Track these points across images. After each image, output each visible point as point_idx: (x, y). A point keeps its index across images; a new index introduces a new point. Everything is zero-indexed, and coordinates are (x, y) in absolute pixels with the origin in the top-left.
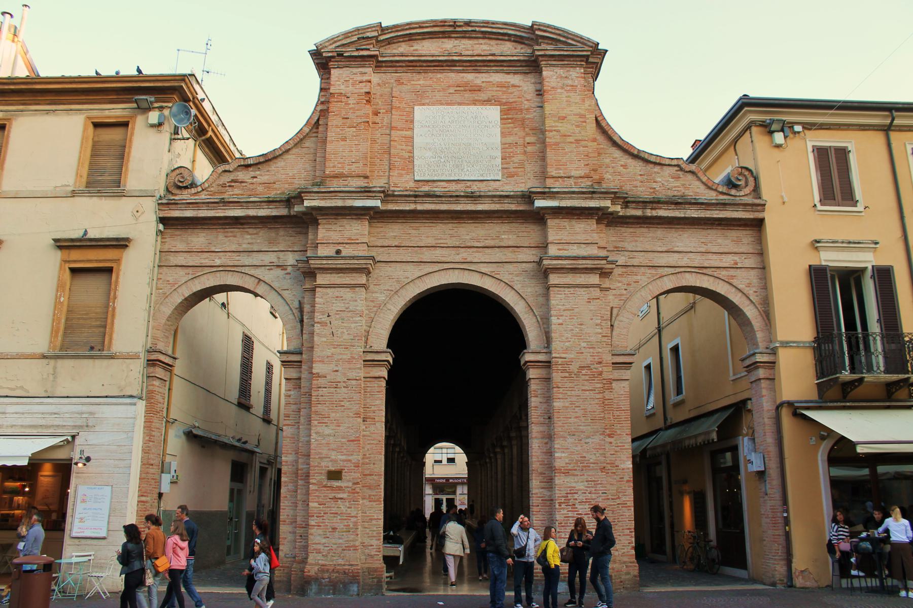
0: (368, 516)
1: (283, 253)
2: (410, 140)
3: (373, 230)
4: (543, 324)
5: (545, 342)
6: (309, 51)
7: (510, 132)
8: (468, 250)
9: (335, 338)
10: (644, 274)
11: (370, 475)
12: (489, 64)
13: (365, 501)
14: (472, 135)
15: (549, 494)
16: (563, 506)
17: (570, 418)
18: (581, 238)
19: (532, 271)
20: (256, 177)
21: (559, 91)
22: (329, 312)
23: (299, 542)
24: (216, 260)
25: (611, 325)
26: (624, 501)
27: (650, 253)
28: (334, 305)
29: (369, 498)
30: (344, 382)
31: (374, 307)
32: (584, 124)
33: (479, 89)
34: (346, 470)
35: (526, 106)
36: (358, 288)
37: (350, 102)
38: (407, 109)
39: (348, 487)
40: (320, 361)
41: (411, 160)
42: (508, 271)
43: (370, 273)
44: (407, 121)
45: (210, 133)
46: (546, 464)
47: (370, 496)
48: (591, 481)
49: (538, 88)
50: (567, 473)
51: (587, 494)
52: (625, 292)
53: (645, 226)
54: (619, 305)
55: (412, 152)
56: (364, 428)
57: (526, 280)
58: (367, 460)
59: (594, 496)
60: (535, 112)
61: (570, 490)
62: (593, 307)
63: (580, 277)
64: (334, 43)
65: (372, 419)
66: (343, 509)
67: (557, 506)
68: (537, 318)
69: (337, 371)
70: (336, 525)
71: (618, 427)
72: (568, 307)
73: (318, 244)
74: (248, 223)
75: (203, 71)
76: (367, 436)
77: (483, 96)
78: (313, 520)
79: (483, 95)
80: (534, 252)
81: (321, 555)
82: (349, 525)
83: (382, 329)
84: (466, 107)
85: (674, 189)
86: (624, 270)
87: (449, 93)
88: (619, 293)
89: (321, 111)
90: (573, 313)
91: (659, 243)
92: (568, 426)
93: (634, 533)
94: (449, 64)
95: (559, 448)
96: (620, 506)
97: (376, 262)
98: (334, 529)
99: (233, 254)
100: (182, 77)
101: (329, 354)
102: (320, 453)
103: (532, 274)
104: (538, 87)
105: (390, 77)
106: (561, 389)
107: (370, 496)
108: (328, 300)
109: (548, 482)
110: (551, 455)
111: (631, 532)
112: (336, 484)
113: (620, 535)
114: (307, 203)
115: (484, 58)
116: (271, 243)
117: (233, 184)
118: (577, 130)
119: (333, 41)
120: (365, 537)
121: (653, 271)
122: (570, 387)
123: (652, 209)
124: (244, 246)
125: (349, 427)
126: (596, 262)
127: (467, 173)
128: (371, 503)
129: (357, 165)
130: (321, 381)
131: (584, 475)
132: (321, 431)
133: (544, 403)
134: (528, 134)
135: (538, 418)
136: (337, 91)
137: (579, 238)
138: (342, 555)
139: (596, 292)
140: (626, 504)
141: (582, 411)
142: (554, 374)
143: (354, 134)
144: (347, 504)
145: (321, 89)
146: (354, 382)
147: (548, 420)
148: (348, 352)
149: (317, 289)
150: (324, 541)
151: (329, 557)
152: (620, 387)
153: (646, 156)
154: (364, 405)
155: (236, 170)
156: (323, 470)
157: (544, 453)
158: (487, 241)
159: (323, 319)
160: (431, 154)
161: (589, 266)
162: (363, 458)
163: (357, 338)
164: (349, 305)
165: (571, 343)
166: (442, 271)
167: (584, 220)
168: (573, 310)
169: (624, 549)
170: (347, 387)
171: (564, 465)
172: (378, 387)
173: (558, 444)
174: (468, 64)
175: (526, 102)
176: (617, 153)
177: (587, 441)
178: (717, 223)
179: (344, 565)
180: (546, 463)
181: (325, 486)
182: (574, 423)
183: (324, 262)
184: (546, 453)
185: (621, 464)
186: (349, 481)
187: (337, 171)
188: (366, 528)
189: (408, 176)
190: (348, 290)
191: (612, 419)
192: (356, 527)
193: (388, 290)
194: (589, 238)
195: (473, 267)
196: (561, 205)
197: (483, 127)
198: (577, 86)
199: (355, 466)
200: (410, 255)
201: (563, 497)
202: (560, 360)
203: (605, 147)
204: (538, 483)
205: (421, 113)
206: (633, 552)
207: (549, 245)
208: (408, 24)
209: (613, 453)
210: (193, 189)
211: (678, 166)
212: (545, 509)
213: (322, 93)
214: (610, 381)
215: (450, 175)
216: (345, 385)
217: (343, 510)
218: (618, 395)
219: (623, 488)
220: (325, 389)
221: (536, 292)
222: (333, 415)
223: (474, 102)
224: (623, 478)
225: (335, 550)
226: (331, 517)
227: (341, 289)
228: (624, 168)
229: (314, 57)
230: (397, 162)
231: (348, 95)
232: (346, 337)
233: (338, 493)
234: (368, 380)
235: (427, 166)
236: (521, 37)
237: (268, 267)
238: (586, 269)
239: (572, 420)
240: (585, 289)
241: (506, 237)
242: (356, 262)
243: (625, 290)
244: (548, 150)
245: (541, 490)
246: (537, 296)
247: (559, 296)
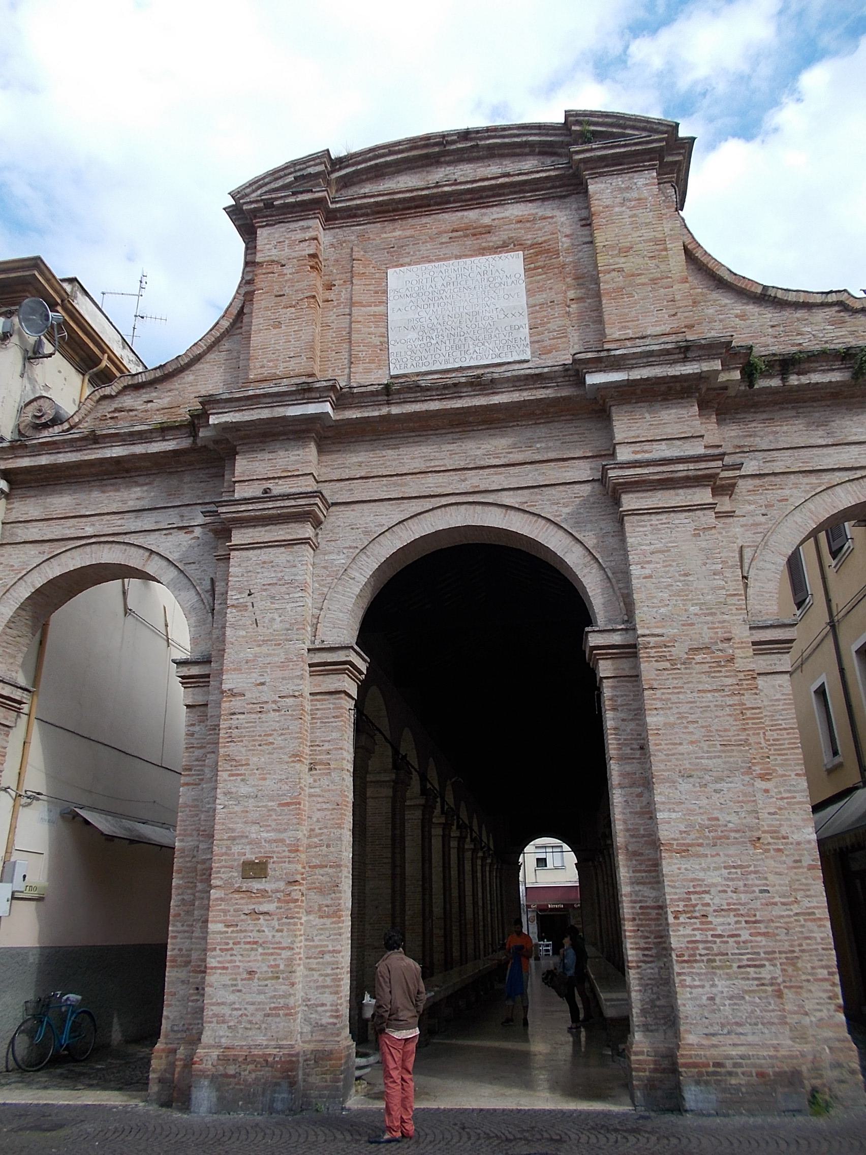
0: (317, 947)
1: (189, 508)
3: (324, 458)
4: (618, 581)
5: (624, 612)
6: (224, 209)
7: (541, 287)
8: (481, 472)
9: (260, 629)
10: (796, 486)
11: (322, 867)
12: (500, 192)
13: (311, 917)
14: (480, 300)
15: (654, 894)
16: (682, 919)
17: (681, 744)
18: (673, 430)
19: (592, 496)
20: (151, 401)
21: (617, 209)
22: (251, 587)
23: (193, 1001)
24: (87, 529)
25: (745, 577)
26: (809, 908)
27: (806, 450)
28: (259, 576)
29: (319, 910)
30: (275, 702)
31: (328, 576)
32: (665, 253)
33: (488, 230)
34: (275, 859)
35: (565, 245)
36: (298, 546)
37: (285, 271)
38: (377, 276)
39: (278, 891)
40: (235, 670)
41: (384, 346)
42: (549, 500)
43: (321, 523)
44: (376, 292)
45: (105, 363)
46: (643, 836)
47: (320, 906)
48: (734, 867)
49: (583, 216)
50: (684, 851)
51: (730, 894)
52: (763, 519)
53: (790, 406)
54: (754, 542)
56: (311, 780)
57: (582, 511)
58: (316, 840)
59: (744, 897)
60: (580, 251)
61: (694, 886)
62: (705, 543)
63: (677, 495)
64: (258, 189)
65: (325, 764)
66: (268, 933)
67: (671, 919)
68: (605, 572)
69: (263, 684)
70: (254, 966)
71: (779, 762)
72: (659, 546)
73: (235, 482)
74: (137, 469)
75: (136, 316)
76: (313, 796)
77: (495, 239)
78: (214, 957)
79: (494, 239)
80: (593, 466)
81: (225, 1026)
82: (278, 966)
83: (341, 612)
84: (468, 260)
86: (757, 482)
87: (442, 243)
88: (751, 522)
89: (246, 294)
90: (669, 556)
91: (820, 433)
92: (677, 759)
93: (837, 977)
94: (439, 200)
95: (663, 803)
96: (801, 918)
97: (329, 506)
98: (251, 973)
99: (114, 517)
100: (33, 262)
101: (251, 657)
102: (233, 830)
103: (591, 499)
104: (584, 214)
105: (350, 234)
106: (659, 692)
107: (320, 906)
108: (250, 568)
109: (650, 871)
110: (651, 818)
111: (830, 974)
112: (256, 885)
113: (808, 981)
114: (213, 420)
115: (493, 182)
116: (170, 495)
117: (116, 415)
118: (652, 264)
119: (257, 185)
120: (310, 988)
121: (813, 479)
122: (675, 688)
123: (798, 374)
124: (131, 503)
125: (281, 780)
126: (703, 465)
127: (474, 356)
128: (322, 920)
129: (297, 360)
130: (237, 704)
131: (718, 854)
132: (234, 790)
133: (632, 720)
135: (620, 749)
136: (267, 259)
137: (669, 430)
138: (263, 1026)
139: (709, 518)
140: (813, 913)
141: (703, 730)
142: (644, 666)
143: (293, 316)
144: (275, 923)
145: (247, 264)
146: (290, 701)
147: (639, 752)
148: (281, 651)
149: (233, 553)
150: (232, 998)
151: (240, 1031)
152: (774, 686)
153: (780, 294)
154: (311, 742)
155: (119, 393)
156: (235, 860)
157: (636, 813)
158: (511, 456)
159: (241, 600)
160: (416, 336)
161: (690, 473)
162: (310, 837)
163: (296, 627)
164: (282, 574)
165: (670, 608)
166: (439, 510)
168: (669, 551)
169: (820, 1010)
170: (278, 711)
171: (678, 836)
172: (334, 708)
173: (661, 794)
174: (469, 196)
175: (564, 239)
176: (725, 300)
177: (718, 786)
179: (267, 1047)
180: (642, 832)
181: (238, 891)
182: (688, 754)
183: (243, 508)
184: (641, 814)
185: (793, 832)
186: (278, 880)
187: (266, 372)
188: (312, 969)
189: (380, 372)
190: (282, 549)
191: (763, 745)
192: (290, 969)
193: (350, 547)
194: (686, 429)
195: (490, 498)
196: (631, 378)
197: (497, 285)
198: (646, 199)
199: (290, 851)
200: (385, 488)
201: (680, 900)
203: (705, 291)
204: (632, 875)
205: (396, 278)
206: (841, 1017)
207: (617, 447)
208: (371, 150)
209: (772, 811)
210: (56, 427)
211: (839, 303)
212: (648, 925)
213: (248, 269)
214: (755, 675)
215: (447, 362)
216: (274, 707)
217: (267, 937)
218: (771, 700)
219: (804, 881)
221: (601, 529)
222: (255, 759)
223: (483, 251)
224: (800, 861)
225: (252, 1015)
226: (247, 950)
227: (270, 549)
228: (744, 320)
229: (234, 217)
230: (362, 352)
231: (283, 262)
232: (277, 626)
233: (260, 903)
234: (318, 697)
235: (409, 353)
237: (165, 532)
238: (687, 478)
240: (687, 514)
241: (543, 445)
242: (293, 503)
243: (763, 515)
244: (604, 302)
245: (637, 888)
246: (603, 537)
247: (641, 529)
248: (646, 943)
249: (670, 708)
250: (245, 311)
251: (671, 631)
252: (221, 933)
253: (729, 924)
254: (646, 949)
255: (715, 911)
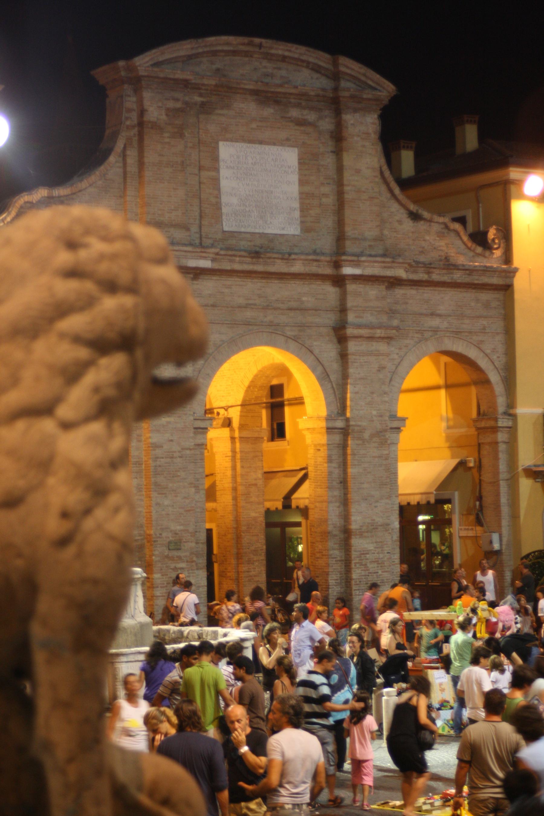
2: (216, 182)
16: (358, 565)
21: (355, 138)
50: (361, 535)
51: (376, 554)
55: (218, 196)
59: (381, 556)
69: (172, 441)
85: (439, 248)
87: (252, 129)
112: (176, 553)
125: (185, 498)
134: (322, 184)
146: (188, 452)
167: (376, 286)
173: (354, 509)
178: (473, 287)
197: (283, 172)
199: (191, 536)
202: (356, 428)
220: (162, 460)
222: (171, 485)
235: (233, 215)
236: (319, 66)
239: (365, 486)
248: (337, 577)
249: (360, 465)
250: (128, 153)
251: (364, 424)
252: (159, 578)
253: (375, 567)
254: (337, 580)
255: (370, 562)
